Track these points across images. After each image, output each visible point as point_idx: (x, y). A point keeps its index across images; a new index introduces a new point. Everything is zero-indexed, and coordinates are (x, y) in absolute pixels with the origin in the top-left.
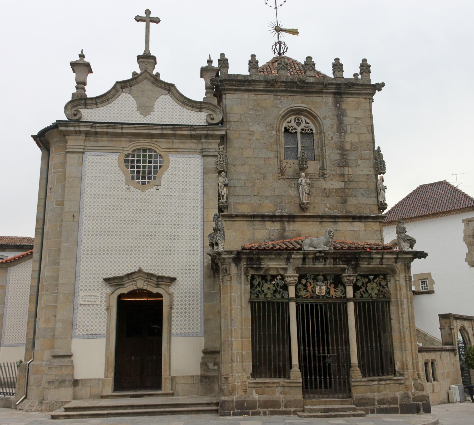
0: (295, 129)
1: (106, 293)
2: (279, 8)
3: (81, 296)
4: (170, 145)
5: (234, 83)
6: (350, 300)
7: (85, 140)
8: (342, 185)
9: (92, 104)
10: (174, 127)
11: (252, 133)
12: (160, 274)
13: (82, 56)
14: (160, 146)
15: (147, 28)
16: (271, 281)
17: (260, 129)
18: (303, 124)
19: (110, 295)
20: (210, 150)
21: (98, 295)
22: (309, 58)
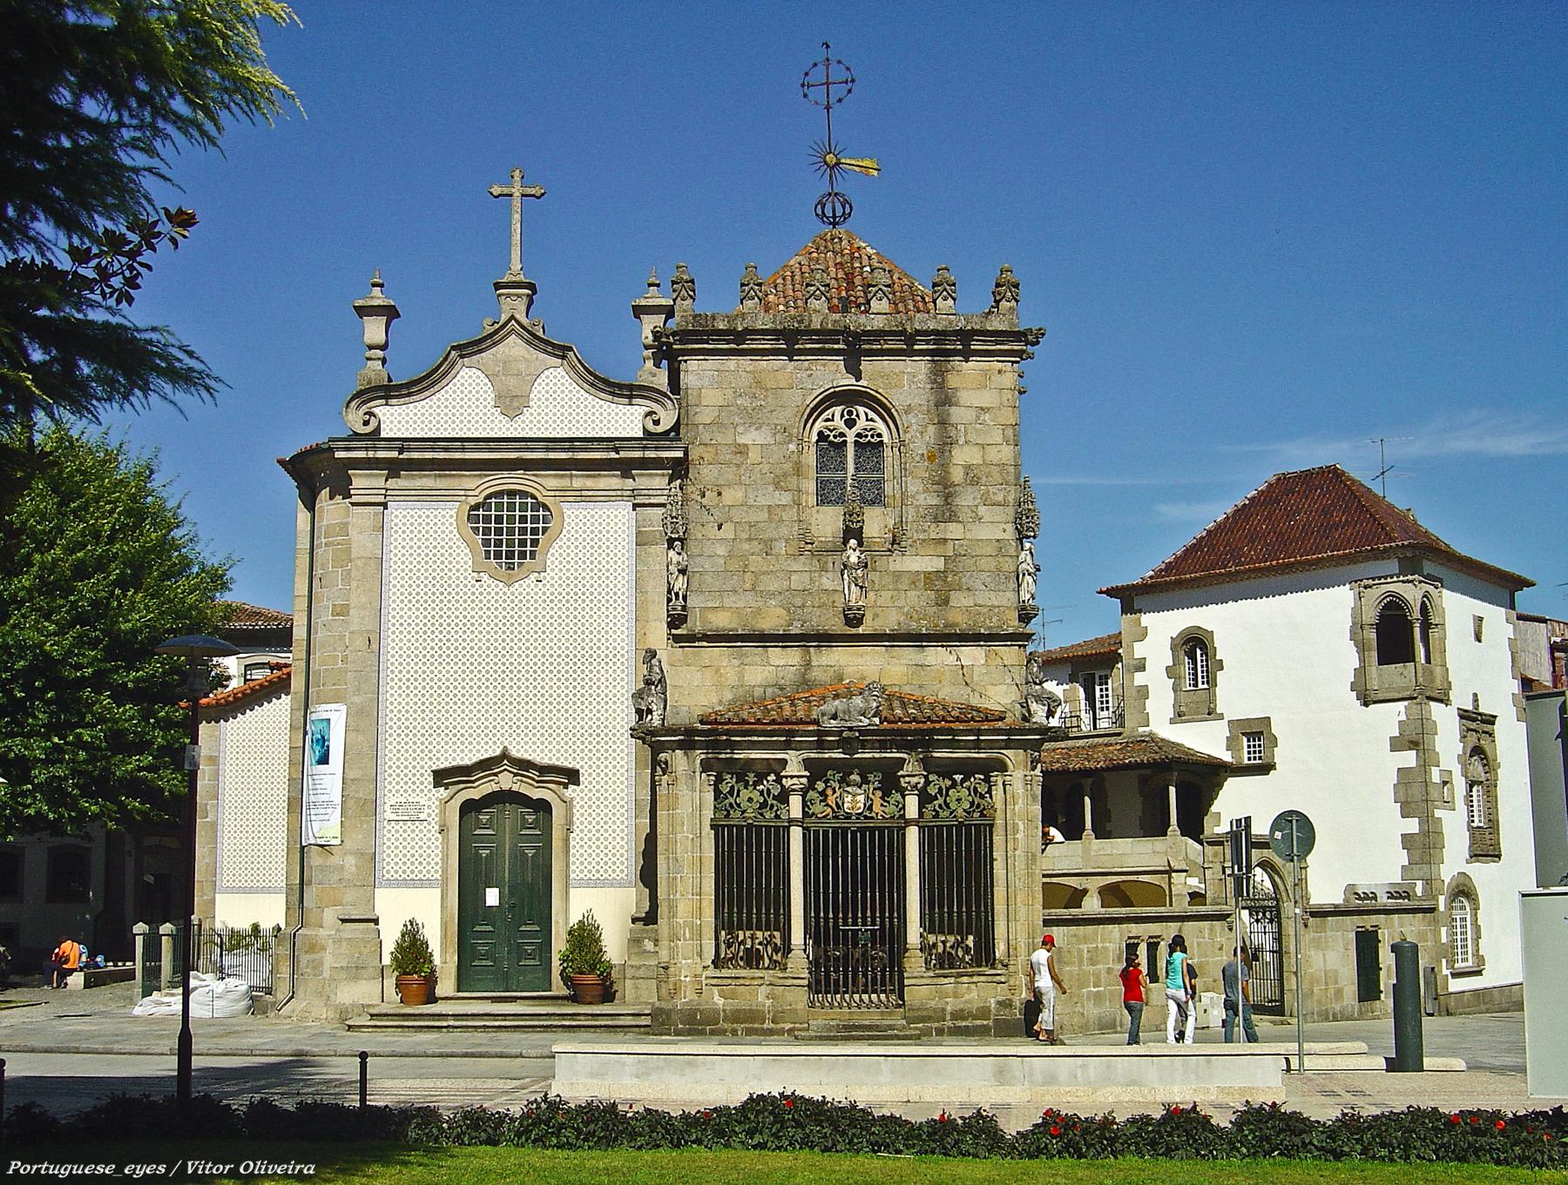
0: (842, 435)
2: (836, 109)
4: (565, 483)
6: (909, 823)
8: (939, 564)
11: (742, 450)
14: (545, 485)
16: (755, 784)
18: (862, 423)
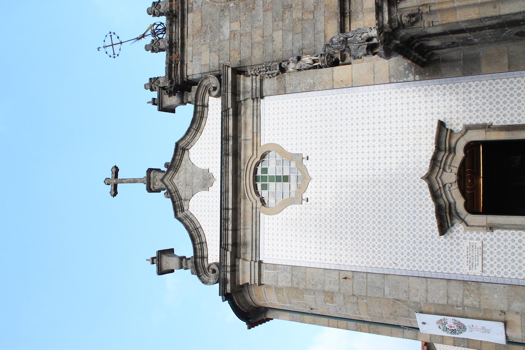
1: (465, 232)
3: (468, 271)
5: (173, 65)
7: (245, 260)
9: (202, 249)
10: (224, 139)
11: (233, 33)
12: (434, 147)
15: (122, 181)
17: (227, 24)
19: (467, 225)
20: (254, 87)
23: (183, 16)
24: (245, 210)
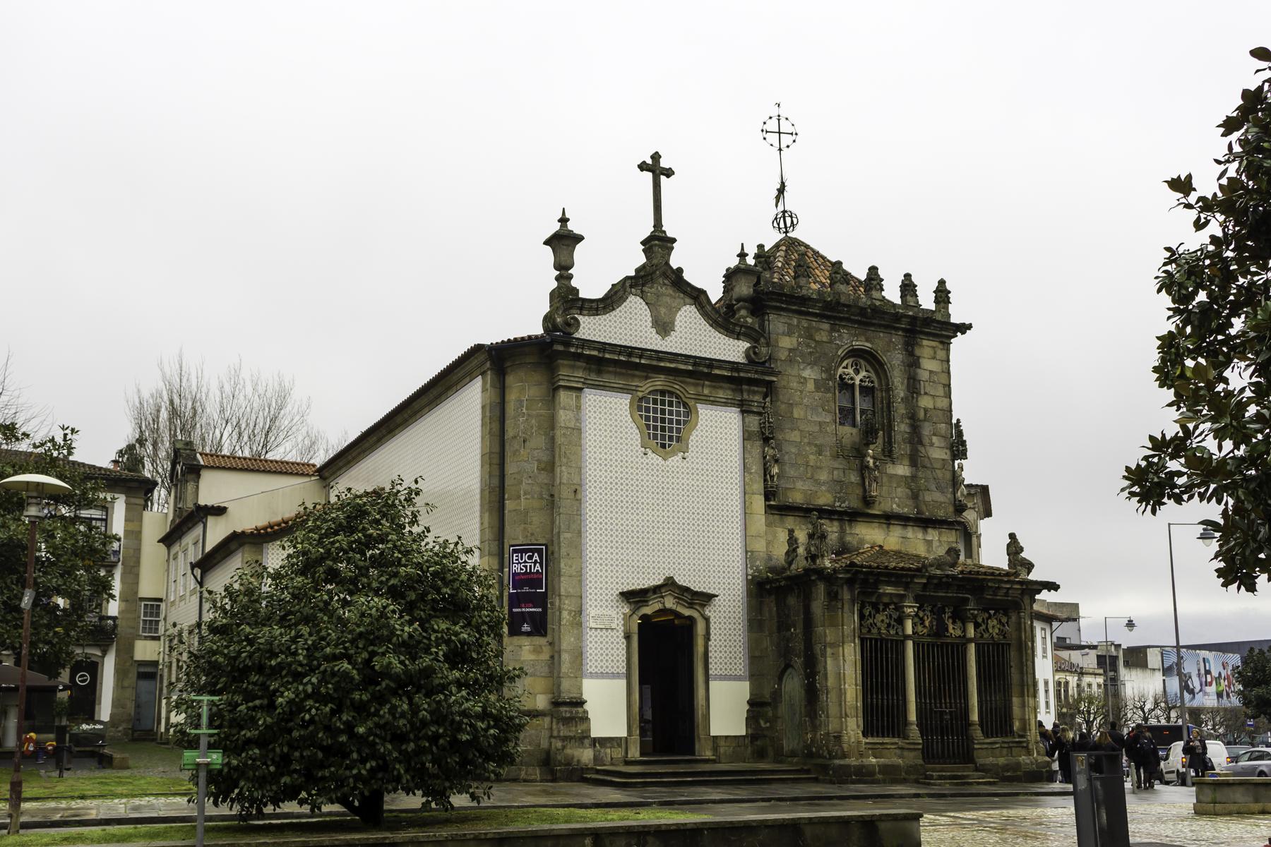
0: (852, 379)
6: (970, 640)
13: (564, 220)
16: (884, 610)
21: (614, 614)
22: (873, 270)
23: (828, 318)
24: (634, 376)
